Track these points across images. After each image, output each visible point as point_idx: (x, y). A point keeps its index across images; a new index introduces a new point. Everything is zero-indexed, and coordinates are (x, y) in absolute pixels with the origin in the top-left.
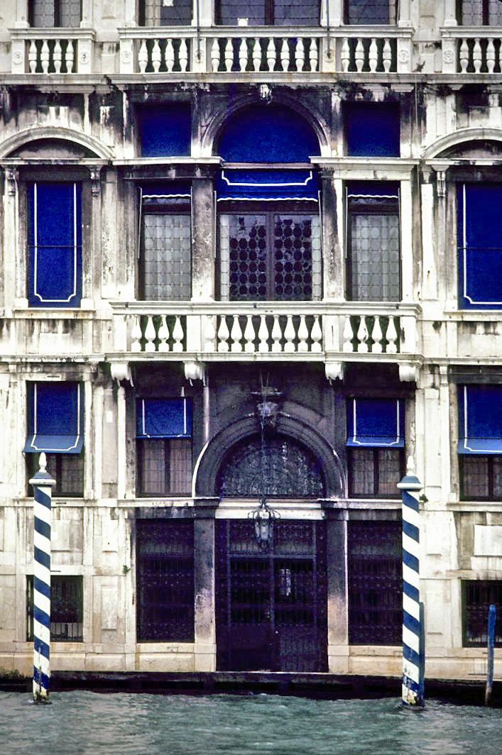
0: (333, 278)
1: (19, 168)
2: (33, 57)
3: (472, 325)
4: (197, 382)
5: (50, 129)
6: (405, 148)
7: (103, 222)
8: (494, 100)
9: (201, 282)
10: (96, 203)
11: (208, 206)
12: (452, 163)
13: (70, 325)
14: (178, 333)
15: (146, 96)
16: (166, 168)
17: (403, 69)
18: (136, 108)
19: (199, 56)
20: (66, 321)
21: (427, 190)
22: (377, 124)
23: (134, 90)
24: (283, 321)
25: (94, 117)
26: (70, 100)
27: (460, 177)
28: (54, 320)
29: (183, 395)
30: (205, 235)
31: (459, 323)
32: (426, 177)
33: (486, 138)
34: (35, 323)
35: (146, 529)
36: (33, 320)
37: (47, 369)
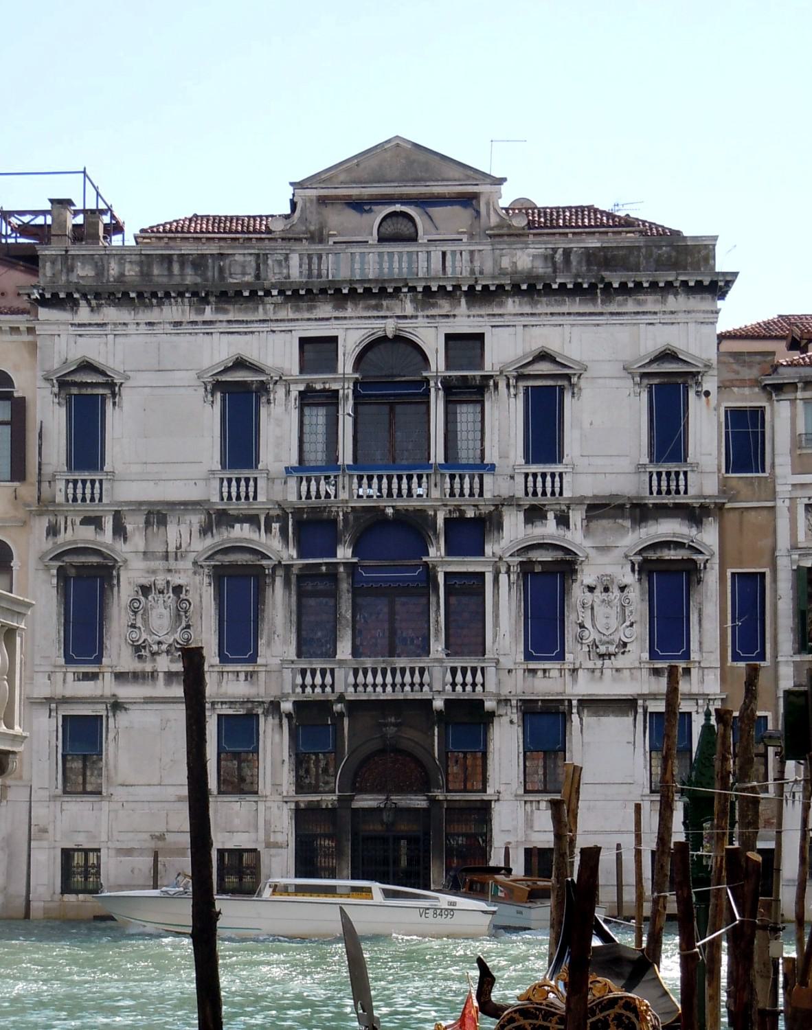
0: (437, 640)
1: (214, 566)
2: (225, 489)
3: (534, 671)
4: (341, 715)
5: (237, 540)
6: (488, 549)
7: (274, 603)
8: (551, 515)
9: (344, 644)
10: (269, 591)
11: (348, 591)
12: (521, 559)
13: (250, 676)
14: (328, 679)
15: (305, 516)
16: (321, 564)
17: (487, 495)
18: (299, 524)
19: (344, 488)
20: (247, 673)
21: (503, 578)
22: (470, 532)
23: (298, 512)
24: (403, 671)
25: (268, 530)
26: (252, 520)
27: (526, 569)
28: (238, 672)
29: (329, 722)
30: (346, 611)
31: (524, 670)
32: (503, 569)
33: (546, 541)
34: (224, 673)
35: (302, 816)
36: (223, 672)
37: (233, 706)
